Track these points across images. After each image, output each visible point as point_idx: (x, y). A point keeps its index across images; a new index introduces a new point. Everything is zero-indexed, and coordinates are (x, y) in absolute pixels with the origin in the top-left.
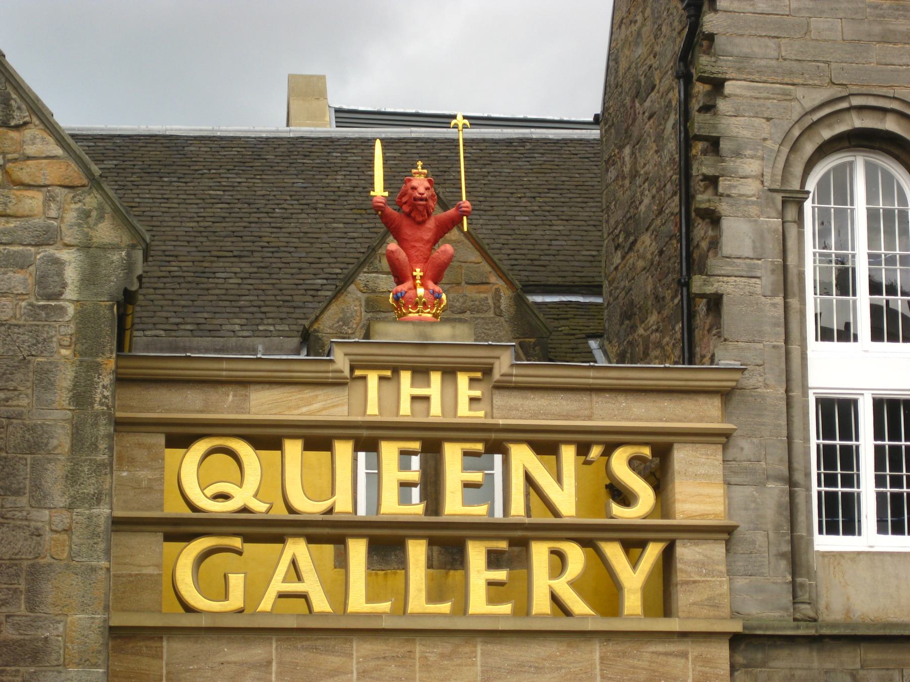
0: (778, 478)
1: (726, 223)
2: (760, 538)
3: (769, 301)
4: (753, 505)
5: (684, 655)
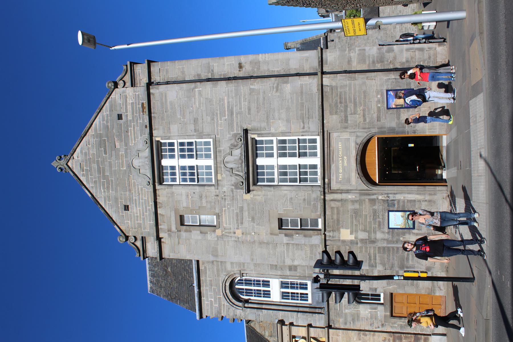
0: (297, 315)
1: (249, 319)
2: (309, 319)
3: (263, 313)
4: (303, 320)
5: (332, 338)
